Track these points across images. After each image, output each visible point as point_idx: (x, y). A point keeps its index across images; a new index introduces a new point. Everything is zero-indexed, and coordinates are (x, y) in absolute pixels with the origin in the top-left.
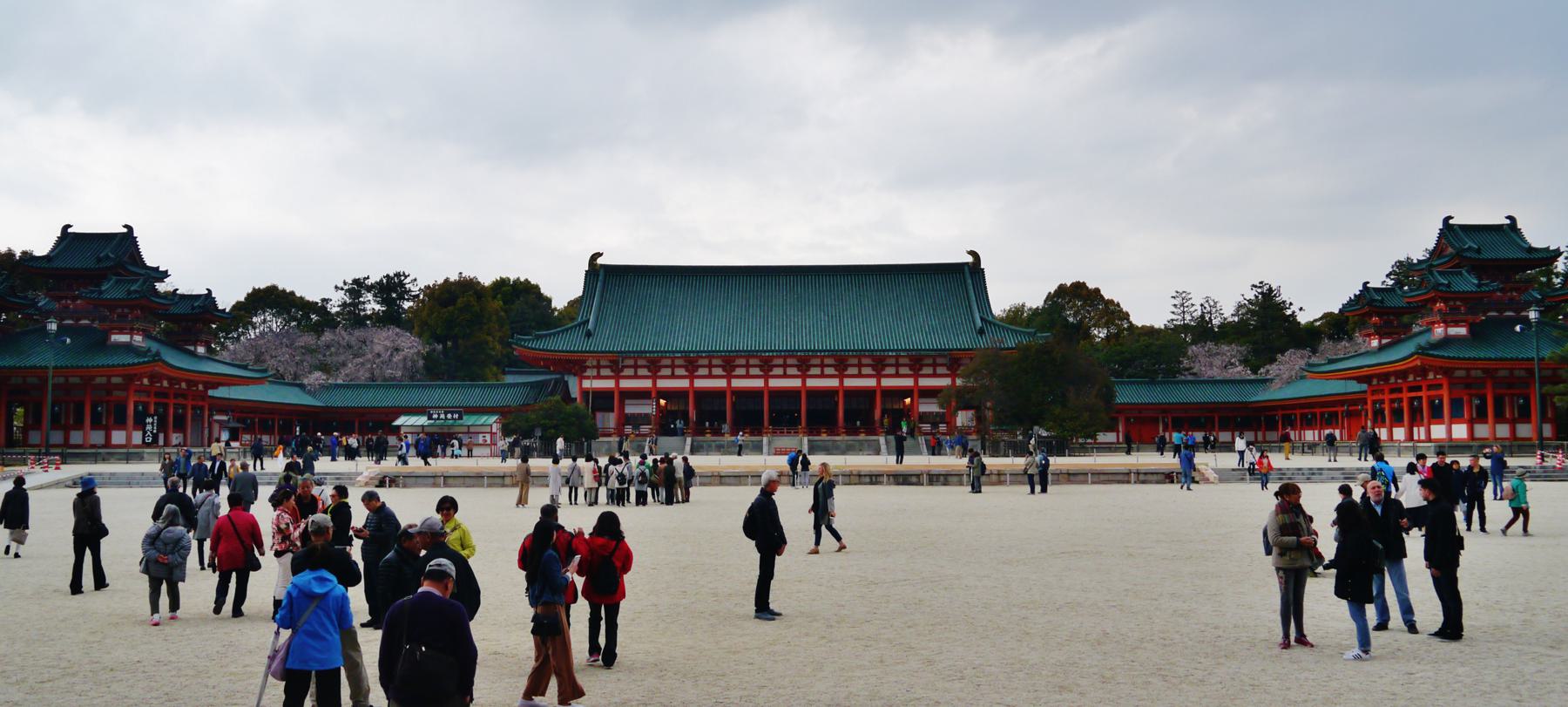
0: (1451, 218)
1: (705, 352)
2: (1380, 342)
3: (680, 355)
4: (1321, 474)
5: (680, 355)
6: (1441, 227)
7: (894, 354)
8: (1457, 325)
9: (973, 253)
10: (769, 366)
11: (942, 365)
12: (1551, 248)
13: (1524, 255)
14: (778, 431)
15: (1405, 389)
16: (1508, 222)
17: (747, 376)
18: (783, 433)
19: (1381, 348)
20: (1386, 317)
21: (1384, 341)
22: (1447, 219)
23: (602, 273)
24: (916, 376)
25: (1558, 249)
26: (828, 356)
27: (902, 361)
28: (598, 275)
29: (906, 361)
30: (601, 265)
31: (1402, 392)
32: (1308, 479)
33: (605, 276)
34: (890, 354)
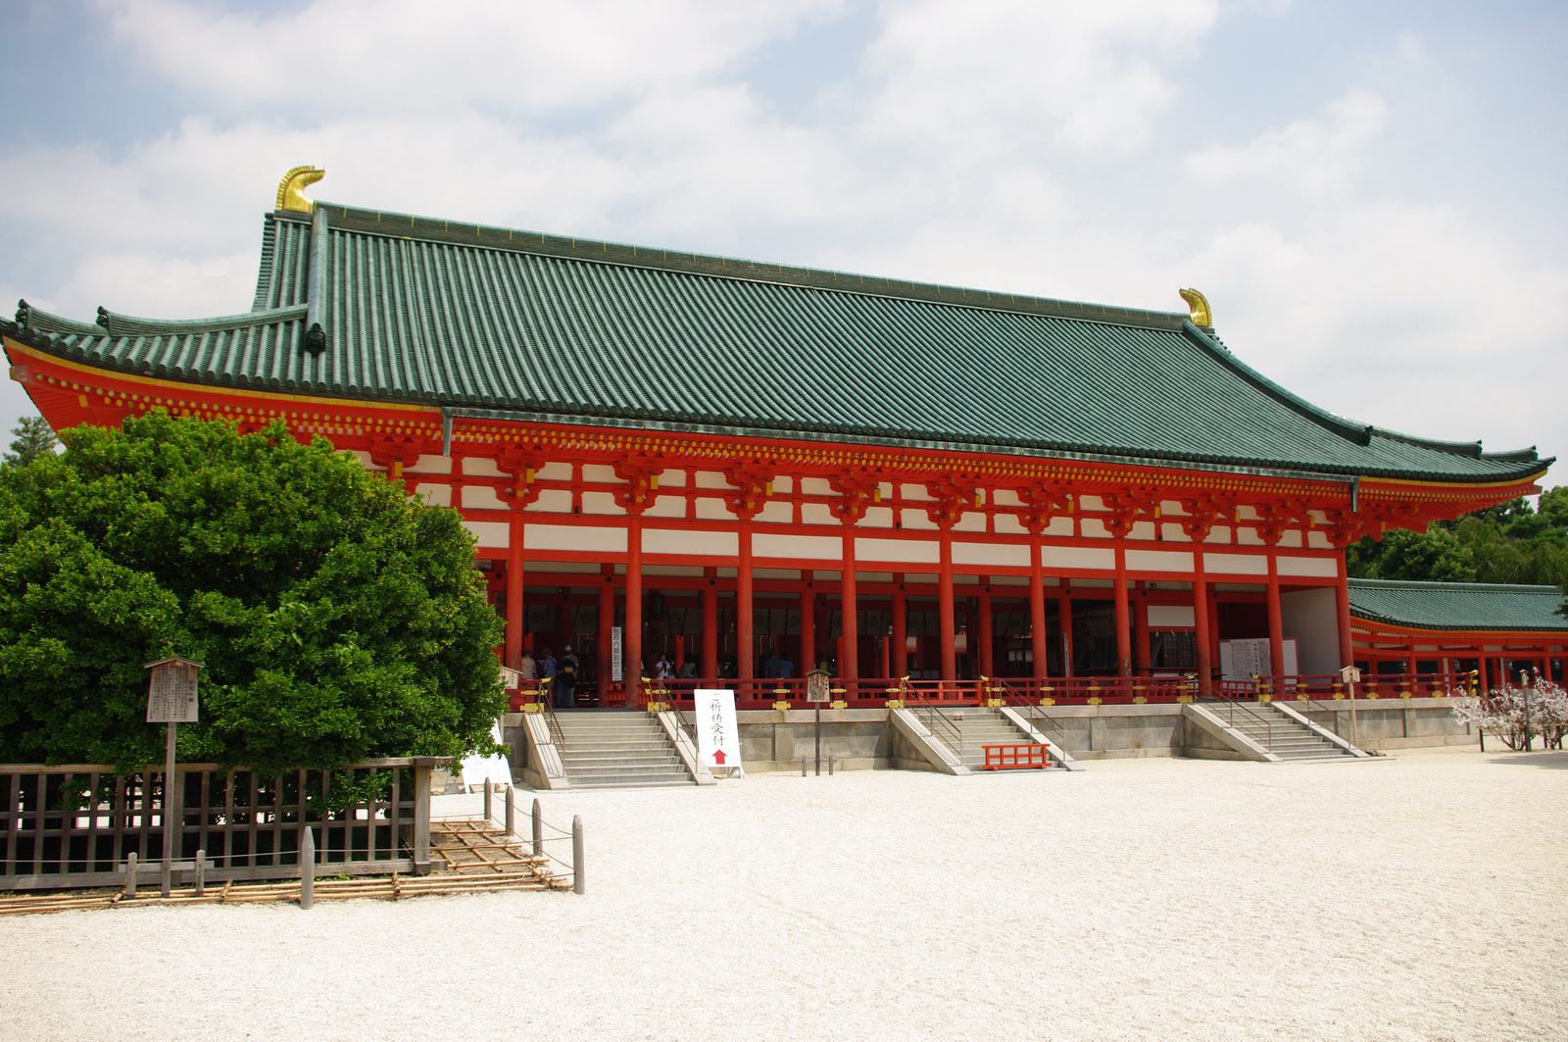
3: (660, 426)
5: (660, 426)
7: (1245, 471)
9: (1191, 298)
14: (921, 692)
17: (797, 528)
18: (934, 695)
23: (321, 227)
28: (309, 228)
30: (318, 206)
33: (331, 232)
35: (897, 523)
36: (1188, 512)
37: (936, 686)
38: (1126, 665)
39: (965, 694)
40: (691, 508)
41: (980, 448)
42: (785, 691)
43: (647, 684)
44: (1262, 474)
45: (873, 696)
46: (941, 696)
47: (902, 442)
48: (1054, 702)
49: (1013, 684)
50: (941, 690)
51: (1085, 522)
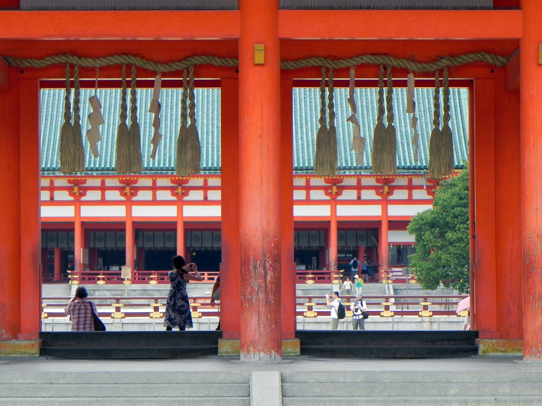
1: (97, 170)
10: (183, 188)
11: (420, 187)
17: (154, 202)
24: (385, 202)
26: (212, 176)
27: (365, 182)
29: (372, 181)
34: (347, 173)
35: (206, 198)
36: (380, 183)
37: (204, 274)
38: (333, 264)
39: (299, 278)
40: (103, 196)
41: (205, 173)
42: (102, 276)
43: (69, 273)
44: (363, 174)
45: (326, 278)
46: (206, 279)
47: (167, 173)
48: (313, 282)
49: (162, 274)
50: (206, 276)
51: (312, 192)
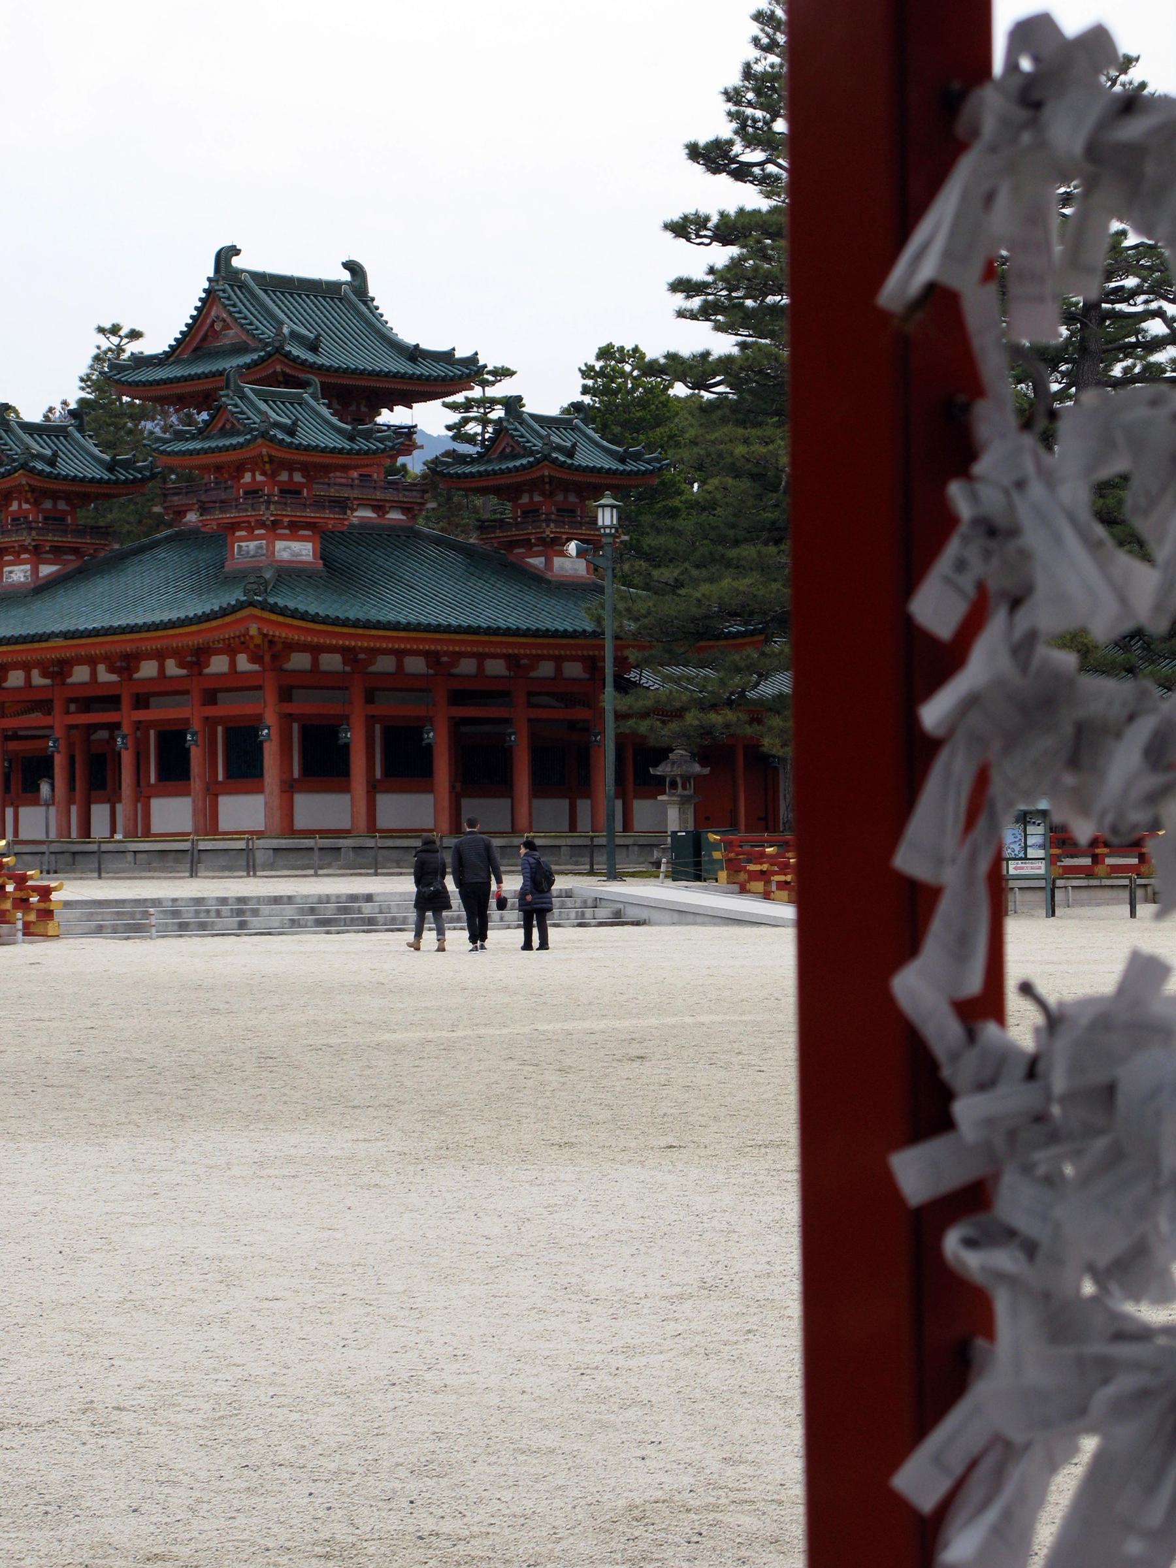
0: (234, 251)
2: (35, 571)
4: (255, 913)
6: (211, 275)
8: (294, 537)
12: (459, 354)
13: (402, 366)
15: (126, 703)
16: (346, 276)
19: (41, 589)
20: (48, 505)
21: (46, 570)
22: (225, 256)
25: (473, 359)
31: (49, 712)
32: (242, 925)
